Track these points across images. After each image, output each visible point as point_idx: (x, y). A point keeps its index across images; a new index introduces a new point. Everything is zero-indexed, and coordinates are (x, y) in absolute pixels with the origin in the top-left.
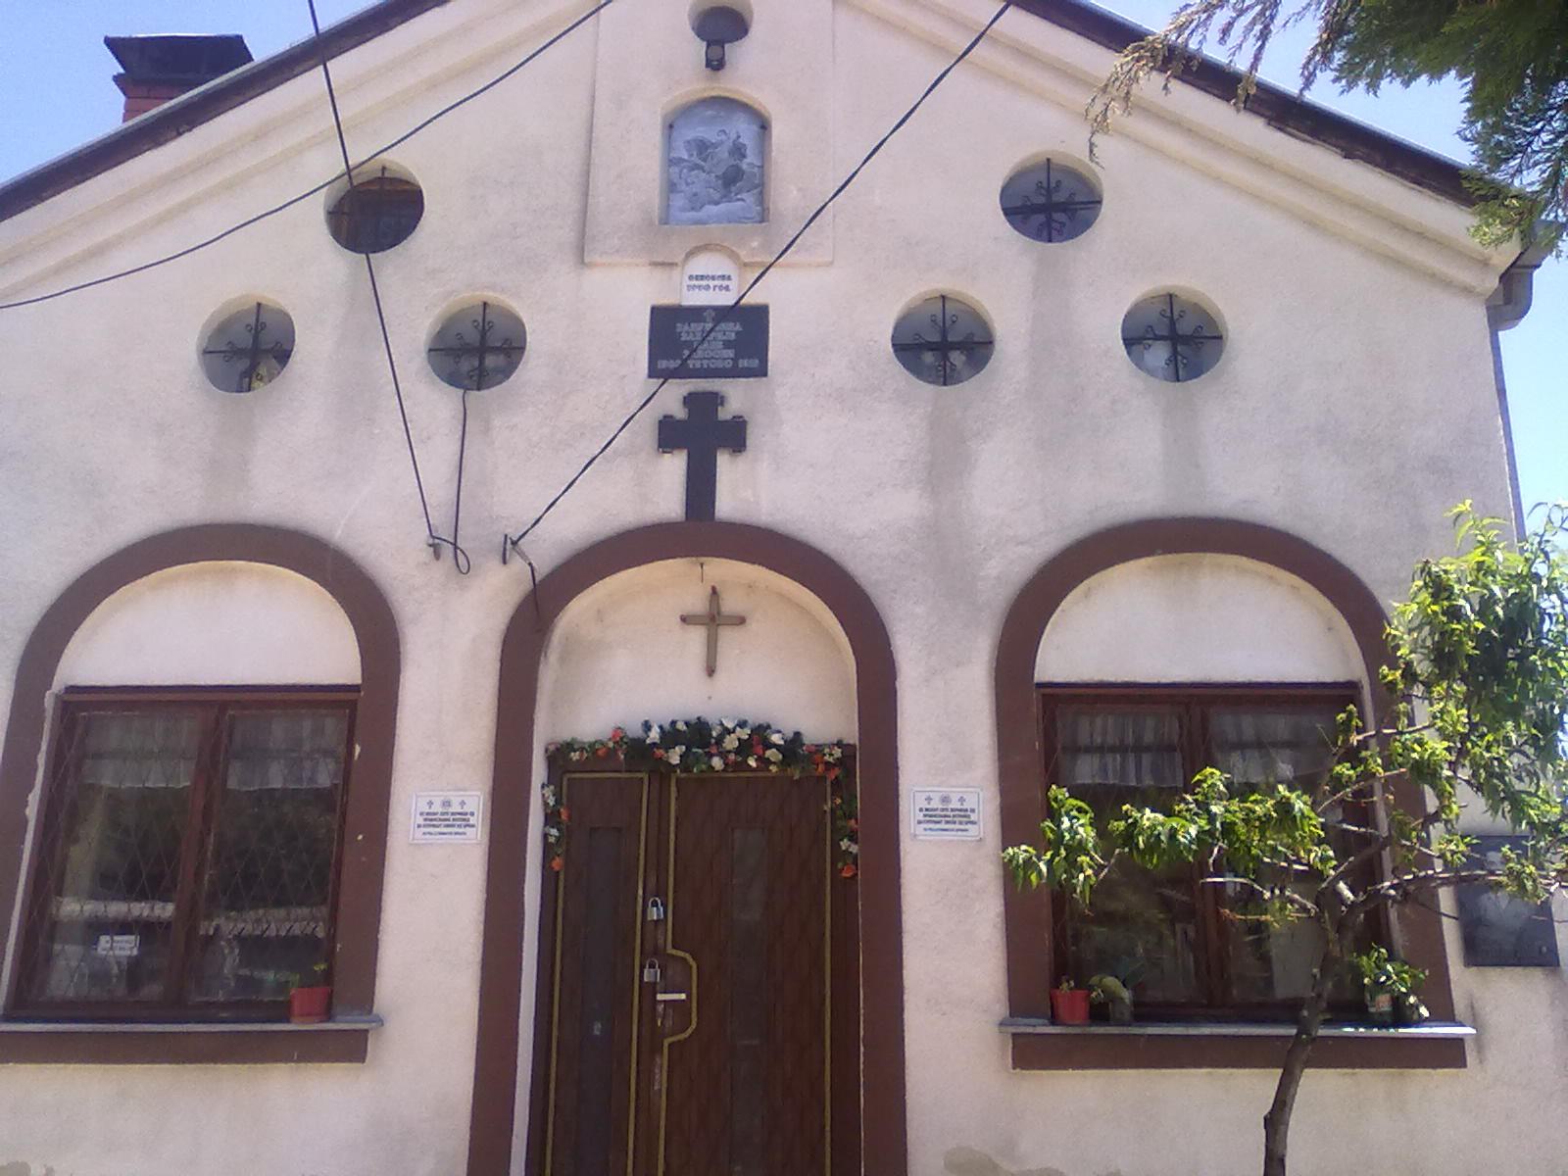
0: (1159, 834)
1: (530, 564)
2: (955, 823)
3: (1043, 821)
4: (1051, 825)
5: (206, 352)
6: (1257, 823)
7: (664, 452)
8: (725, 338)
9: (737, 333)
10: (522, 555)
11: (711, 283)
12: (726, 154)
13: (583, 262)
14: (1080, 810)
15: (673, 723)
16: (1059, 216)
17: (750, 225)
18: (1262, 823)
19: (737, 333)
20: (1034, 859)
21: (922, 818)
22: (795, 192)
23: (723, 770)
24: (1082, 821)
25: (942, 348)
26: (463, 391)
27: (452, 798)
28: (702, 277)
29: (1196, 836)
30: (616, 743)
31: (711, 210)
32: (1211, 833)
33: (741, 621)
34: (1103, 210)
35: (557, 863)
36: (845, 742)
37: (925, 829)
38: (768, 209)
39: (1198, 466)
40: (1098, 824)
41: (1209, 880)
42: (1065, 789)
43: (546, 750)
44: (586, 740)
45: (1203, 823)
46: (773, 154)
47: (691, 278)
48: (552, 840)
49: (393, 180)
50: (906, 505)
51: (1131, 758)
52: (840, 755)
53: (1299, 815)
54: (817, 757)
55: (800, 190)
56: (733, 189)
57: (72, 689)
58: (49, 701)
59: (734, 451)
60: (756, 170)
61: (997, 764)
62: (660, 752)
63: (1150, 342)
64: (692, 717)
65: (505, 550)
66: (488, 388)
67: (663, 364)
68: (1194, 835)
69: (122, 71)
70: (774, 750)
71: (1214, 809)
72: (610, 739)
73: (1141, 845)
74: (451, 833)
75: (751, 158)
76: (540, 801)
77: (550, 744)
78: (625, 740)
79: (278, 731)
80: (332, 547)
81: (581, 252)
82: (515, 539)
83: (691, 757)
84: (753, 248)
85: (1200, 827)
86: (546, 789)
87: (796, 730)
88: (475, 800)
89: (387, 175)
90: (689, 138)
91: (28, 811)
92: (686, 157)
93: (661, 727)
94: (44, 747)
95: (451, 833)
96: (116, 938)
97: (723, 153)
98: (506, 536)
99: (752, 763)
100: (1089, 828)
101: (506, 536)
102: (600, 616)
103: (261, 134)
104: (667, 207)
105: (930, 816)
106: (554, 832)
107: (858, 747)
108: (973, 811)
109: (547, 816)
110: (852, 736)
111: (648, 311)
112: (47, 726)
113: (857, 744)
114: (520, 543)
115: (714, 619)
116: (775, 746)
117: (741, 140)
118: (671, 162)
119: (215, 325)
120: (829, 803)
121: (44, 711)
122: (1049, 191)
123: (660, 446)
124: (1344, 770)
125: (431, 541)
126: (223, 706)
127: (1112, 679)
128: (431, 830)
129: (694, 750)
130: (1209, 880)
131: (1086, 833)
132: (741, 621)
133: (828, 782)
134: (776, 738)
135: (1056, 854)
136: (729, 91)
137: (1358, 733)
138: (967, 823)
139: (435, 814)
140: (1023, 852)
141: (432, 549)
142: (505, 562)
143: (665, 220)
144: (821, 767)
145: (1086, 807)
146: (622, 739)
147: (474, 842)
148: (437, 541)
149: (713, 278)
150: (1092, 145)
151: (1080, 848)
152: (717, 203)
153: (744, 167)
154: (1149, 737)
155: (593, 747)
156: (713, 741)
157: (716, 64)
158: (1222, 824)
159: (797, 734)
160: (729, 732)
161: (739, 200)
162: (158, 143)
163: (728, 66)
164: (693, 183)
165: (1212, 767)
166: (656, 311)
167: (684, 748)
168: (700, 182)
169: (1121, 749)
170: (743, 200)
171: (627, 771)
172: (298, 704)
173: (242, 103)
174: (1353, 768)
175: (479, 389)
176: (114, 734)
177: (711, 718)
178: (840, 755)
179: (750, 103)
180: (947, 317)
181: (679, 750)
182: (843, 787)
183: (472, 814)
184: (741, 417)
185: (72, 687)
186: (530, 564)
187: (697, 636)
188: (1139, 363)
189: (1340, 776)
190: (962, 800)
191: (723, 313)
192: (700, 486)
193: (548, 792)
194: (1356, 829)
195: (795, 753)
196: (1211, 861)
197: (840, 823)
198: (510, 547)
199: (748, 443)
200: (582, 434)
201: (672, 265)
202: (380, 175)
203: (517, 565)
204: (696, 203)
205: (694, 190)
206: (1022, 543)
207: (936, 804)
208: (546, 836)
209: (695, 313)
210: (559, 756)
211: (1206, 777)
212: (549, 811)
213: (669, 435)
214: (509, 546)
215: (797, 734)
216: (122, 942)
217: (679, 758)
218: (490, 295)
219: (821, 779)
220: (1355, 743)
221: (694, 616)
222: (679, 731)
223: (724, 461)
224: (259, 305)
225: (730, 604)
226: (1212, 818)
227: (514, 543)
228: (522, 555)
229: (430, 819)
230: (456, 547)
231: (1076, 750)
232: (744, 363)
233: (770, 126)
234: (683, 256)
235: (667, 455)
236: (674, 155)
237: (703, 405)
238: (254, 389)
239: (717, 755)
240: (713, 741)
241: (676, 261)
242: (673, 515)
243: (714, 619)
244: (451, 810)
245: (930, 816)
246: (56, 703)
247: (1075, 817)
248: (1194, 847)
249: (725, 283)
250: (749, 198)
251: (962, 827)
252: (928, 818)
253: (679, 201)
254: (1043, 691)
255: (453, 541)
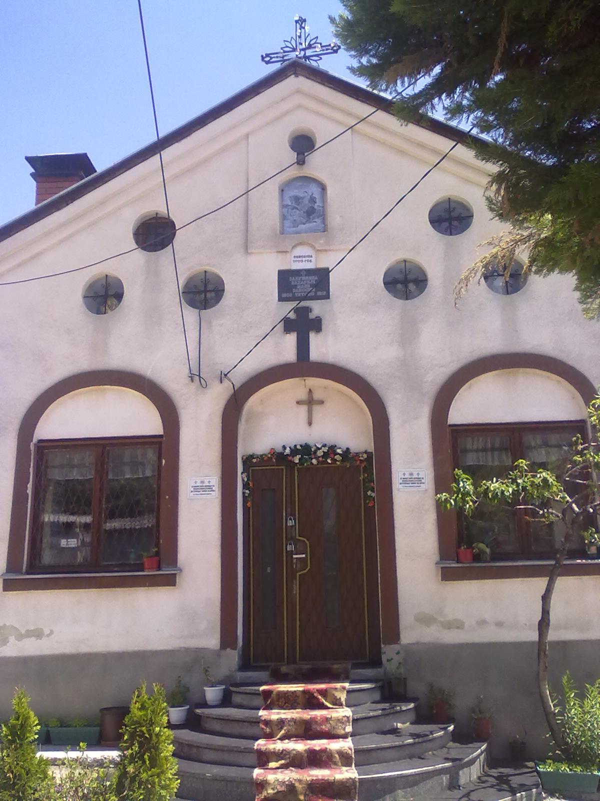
0: (497, 493)
1: (232, 383)
2: (415, 483)
3: (453, 483)
4: (455, 485)
5: (85, 297)
6: (536, 486)
7: (287, 333)
8: (311, 283)
9: (316, 281)
10: (229, 380)
11: (304, 259)
12: (307, 202)
13: (247, 252)
14: (467, 479)
15: (295, 446)
16: (455, 223)
17: (319, 233)
18: (537, 486)
19: (316, 281)
20: (449, 499)
21: (401, 482)
22: (338, 218)
23: (317, 464)
24: (468, 483)
25: (405, 282)
26: (198, 310)
27: (205, 480)
28: (300, 257)
29: (512, 492)
30: (272, 455)
31: (302, 227)
32: (518, 491)
33: (322, 402)
34: (474, 220)
35: (249, 504)
36: (368, 451)
37: (403, 487)
38: (327, 225)
39: (517, 331)
40: (476, 485)
41: (518, 507)
42: (461, 471)
43: (242, 458)
44: (259, 454)
45: (514, 487)
46: (328, 201)
47: (294, 257)
48: (247, 495)
49: (160, 218)
50: (391, 352)
51: (489, 454)
52: (366, 457)
53: (551, 484)
54: (356, 458)
55: (341, 217)
56: (311, 217)
57: (41, 441)
58: (32, 447)
59: (317, 332)
60: (321, 208)
61: (432, 460)
62: (290, 458)
63: (496, 277)
64: (303, 443)
65: (221, 377)
66: (210, 308)
67: (284, 295)
68: (511, 492)
69: (34, 171)
70: (338, 456)
71: (519, 481)
72: (269, 454)
73: (490, 496)
74: (204, 494)
75: (319, 203)
76: (241, 480)
77: (244, 456)
78: (275, 453)
79: (127, 453)
80: (146, 378)
81: (246, 247)
82: (226, 373)
83: (304, 459)
84: (320, 243)
85: (513, 489)
86: (243, 474)
87: (347, 447)
88: (215, 481)
89: (158, 216)
90: (290, 195)
91: (28, 491)
92: (290, 204)
93: (290, 448)
94: (32, 465)
95: (204, 494)
96: (69, 540)
97: (306, 201)
98: (221, 372)
99: (329, 461)
100: (471, 486)
101: (221, 372)
102: (262, 402)
103: (103, 202)
104: (282, 226)
105: (405, 481)
106: (247, 491)
107: (374, 454)
108: (423, 478)
109: (244, 485)
110: (371, 449)
111: (277, 272)
112: (32, 457)
113: (373, 452)
114: (228, 375)
115: (310, 402)
116: (339, 454)
117: (314, 195)
118: (283, 206)
119: (88, 285)
120: (362, 477)
121: (31, 450)
122: (450, 212)
123: (285, 331)
124: (577, 458)
125: (190, 375)
126: (104, 446)
127: (481, 422)
128: (197, 493)
129: (305, 457)
130: (518, 507)
131: (470, 488)
132: (322, 402)
133: (362, 468)
134: (339, 451)
135: (458, 496)
136: (310, 174)
137: (582, 445)
138: (421, 483)
139: (198, 486)
140: (444, 496)
141: (190, 378)
142: (221, 382)
143: (282, 233)
144: (358, 462)
145: (470, 478)
146: (274, 453)
147: (214, 500)
148: (192, 375)
149: (305, 257)
150: (456, 304)
151: (468, 494)
152: (304, 224)
153: (316, 207)
154: (497, 445)
155: (261, 457)
156: (312, 453)
157: (301, 162)
158: (522, 487)
159: (348, 449)
160: (319, 449)
161: (314, 222)
162: (59, 209)
163: (306, 165)
164: (294, 215)
165: (521, 459)
166: (281, 273)
167: (300, 456)
168: (297, 215)
169: (484, 450)
170: (316, 222)
171: (277, 466)
172: (137, 444)
173: (94, 189)
174: (581, 457)
175: (205, 309)
176: (56, 458)
177: (311, 443)
178: (366, 457)
179: (317, 179)
180: (407, 270)
181: (299, 456)
182: (368, 469)
183: (214, 486)
184: (319, 317)
185: (40, 440)
186: (232, 383)
187: (304, 409)
188: (491, 286)
189: (576, 460)
190: (418, 474)
191: (309, 272)
192: (303, 347)
193: (244, 475)
194: (582, 482)
195: (347, 456)
196: (521, 498)
197: (367, 484)
198: (223, 377)
199: (323, 328)
200: (251, 327)
201: (286, 252)
202: (155, 216)
203: (226, 383)
204: (295, 224)
205: (295, 219)
206: (442, 367)
207: (407, 476)
208: (244, 493)
209: (297, 273)
210: (248, 460)
211: (519, 463)
212: (245, 483)
213: (288, 325)
214: (223, 375)
215: (348, 449)
216: (296, 588)
217: (298, 460)
218: (207, 268)
219: (358, 467)
220: (580, 449)
221: (301, 401)
222: (298, 449)
223: (312, 336)
224: (107, 276)
225: (317, 396)
226: (518, 484)
227: (226, 375)
228: (229, 380)
229: (196, 489)
230: (200, 377)
231: (465, 451)
232: (319, 293)
233: (326, 188)
234: (291, 247)
235: (288, 335)
236: (285, 203)
237: (303, 312)
238: (107, 313)
239: (314, 458)
240: (312, 453)
241: (288, 250)
242: (292, 360)
243: (310, 402)
244: (204, 485)
245: (405, 481)
246: (35, 447)
247: (465, 482)
248: (511, 496)
249: (310, 259)
250: (319, 221)
251: (418, 485)
252: (404, 482)
253: (287, 223)
254: (452, 428)
255: (198, 374)
